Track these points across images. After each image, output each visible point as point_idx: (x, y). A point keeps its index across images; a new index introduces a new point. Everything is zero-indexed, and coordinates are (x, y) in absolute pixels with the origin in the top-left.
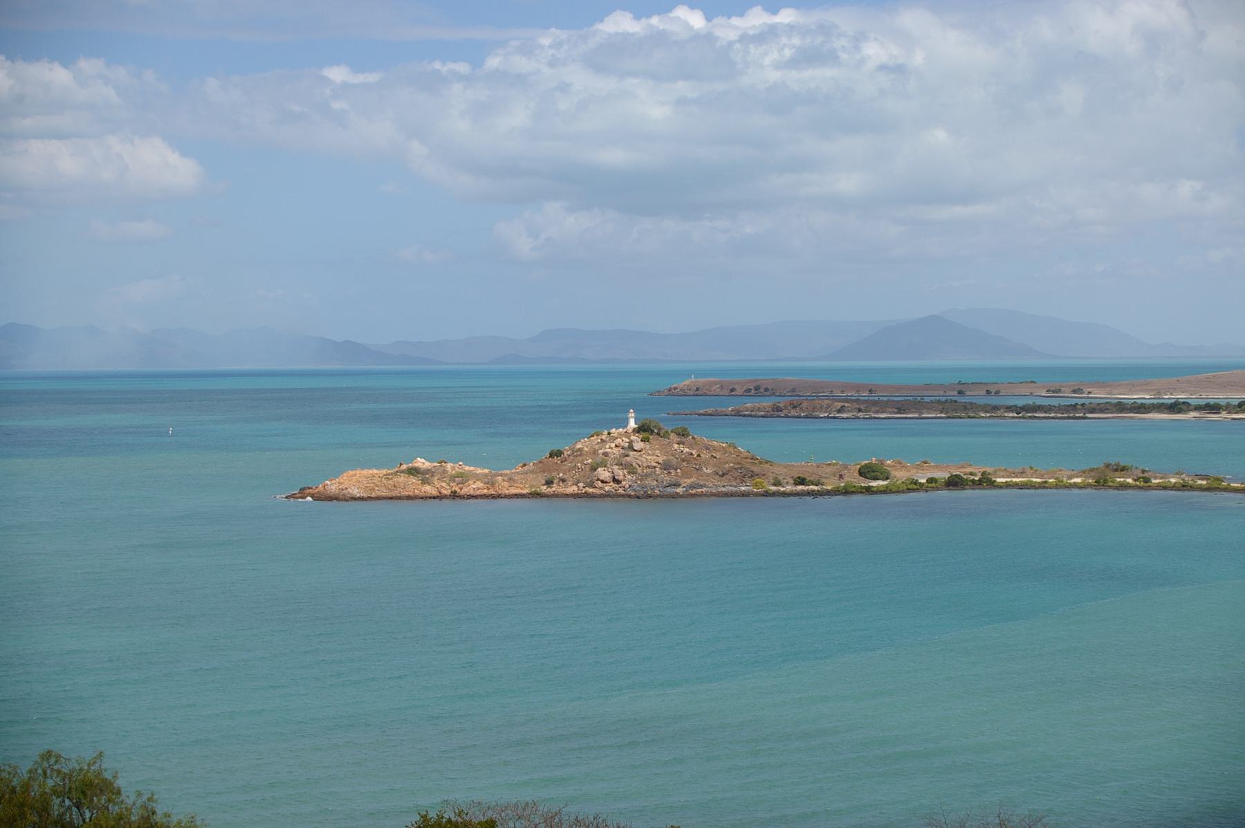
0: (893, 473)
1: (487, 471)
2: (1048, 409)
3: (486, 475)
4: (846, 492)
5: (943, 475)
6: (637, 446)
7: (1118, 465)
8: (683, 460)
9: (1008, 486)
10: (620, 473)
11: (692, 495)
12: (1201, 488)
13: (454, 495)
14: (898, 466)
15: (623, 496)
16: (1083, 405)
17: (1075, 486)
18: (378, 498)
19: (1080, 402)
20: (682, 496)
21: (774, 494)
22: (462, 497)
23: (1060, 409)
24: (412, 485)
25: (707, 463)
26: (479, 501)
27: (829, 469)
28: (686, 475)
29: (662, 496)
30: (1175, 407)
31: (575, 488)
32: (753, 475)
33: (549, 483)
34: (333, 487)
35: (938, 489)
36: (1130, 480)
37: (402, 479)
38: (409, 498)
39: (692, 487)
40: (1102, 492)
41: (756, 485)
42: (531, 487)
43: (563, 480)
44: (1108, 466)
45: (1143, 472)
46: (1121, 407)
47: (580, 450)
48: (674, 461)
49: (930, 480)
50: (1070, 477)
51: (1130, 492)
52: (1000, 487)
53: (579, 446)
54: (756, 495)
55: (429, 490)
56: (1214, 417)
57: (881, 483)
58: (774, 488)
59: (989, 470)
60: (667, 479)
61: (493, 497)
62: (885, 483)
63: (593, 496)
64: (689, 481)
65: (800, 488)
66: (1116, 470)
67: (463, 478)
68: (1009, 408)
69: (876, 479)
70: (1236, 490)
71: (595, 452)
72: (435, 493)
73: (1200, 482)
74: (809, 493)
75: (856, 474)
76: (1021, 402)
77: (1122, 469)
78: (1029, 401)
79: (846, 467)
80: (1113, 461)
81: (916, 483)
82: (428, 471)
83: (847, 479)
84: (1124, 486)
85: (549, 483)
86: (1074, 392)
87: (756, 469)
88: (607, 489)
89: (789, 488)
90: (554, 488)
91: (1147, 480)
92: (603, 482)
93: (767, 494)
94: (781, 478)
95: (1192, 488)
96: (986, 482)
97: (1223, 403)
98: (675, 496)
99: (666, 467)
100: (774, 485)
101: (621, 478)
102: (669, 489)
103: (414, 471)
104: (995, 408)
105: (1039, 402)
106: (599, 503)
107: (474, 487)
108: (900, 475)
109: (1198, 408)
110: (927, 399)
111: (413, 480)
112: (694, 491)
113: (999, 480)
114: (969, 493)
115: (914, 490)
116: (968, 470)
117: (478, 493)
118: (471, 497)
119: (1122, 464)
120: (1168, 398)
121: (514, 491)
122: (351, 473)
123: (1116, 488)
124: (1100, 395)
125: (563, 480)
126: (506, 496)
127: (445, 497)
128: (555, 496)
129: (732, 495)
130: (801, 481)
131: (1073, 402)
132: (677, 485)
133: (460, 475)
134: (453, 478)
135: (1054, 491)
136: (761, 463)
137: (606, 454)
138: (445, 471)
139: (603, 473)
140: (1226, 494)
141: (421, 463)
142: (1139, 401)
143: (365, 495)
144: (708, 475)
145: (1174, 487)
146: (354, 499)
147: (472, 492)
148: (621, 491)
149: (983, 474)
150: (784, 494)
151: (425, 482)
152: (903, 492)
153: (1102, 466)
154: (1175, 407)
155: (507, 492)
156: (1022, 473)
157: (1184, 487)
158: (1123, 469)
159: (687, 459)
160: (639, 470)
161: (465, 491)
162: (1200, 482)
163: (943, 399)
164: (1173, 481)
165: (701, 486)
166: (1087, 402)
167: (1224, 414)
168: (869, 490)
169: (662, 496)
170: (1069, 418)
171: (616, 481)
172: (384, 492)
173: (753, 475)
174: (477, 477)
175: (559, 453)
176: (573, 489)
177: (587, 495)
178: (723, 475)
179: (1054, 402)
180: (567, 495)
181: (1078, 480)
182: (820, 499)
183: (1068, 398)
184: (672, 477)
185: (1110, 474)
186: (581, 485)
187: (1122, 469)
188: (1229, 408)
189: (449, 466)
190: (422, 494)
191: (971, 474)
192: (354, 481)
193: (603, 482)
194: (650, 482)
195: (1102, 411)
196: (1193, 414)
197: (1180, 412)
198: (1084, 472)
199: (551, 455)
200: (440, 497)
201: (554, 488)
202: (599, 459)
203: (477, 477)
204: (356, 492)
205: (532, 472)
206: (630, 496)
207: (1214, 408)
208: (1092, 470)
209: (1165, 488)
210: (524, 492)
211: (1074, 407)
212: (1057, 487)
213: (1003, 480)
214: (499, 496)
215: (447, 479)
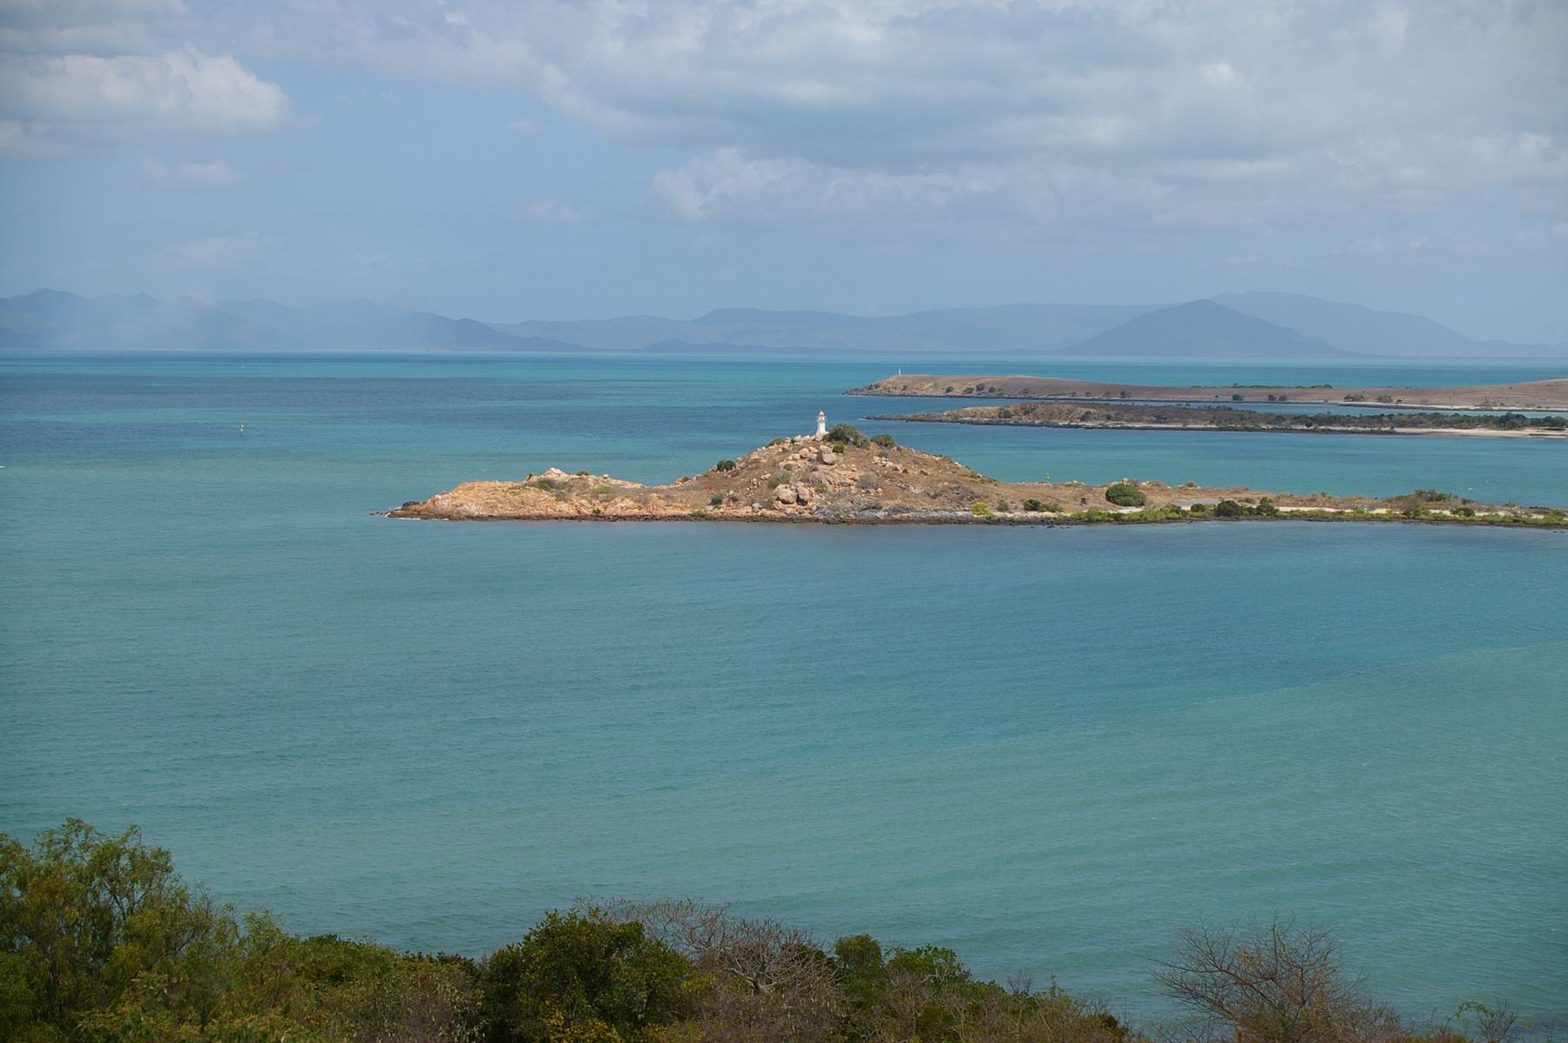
0: (1150, 497)
1: (638, 486)
2: (1347, 421)
3: (637, 491)
4: (1090, 520)
5: (1212, 501)
6: (828, 458)
7: (1432, 493)
8: (886, 477)
9: (1293, 516)
10: (806, 492)
11: (897, 521)
12: (1537, 525)
13: (597, 516)
15: (809, 520)
17: (1379, 518)
18: (501, 518)
19: (1387, 412)
20: (883, 522)
21: (999, 521)
22: (607, 518)
23: (1362, 421)
24: (544, 502)
25: (915, 481)
27: (1069, 492)
34: (444, 502)
36: (1447, 513)
37: (532, 494)
38: (540, 518)
39: (896, 510)
41: (976, 510)
42: (694, 506)
43: (735, 500)
44: (1420, 494)
45: (1464, 502)
47: (756, 461)
48: (874, 478)
49: (1196, 508)
50: (1373, 507)
51: (1447, 527)
52: (1284, 517)
53: (755, 456)
54: (977, 522)
55: (565, 508)
57: (1134, 510)
58: (999, 514)
59: (1270, 496)
60: (865, 500)
61: (646, 518)
62: (1139, 510)
63: (772, 520)
64: (892, 503)
65: (1032, 514)
66: (1431, 500)
67: (609, 494)
68: (1297, 419)
69: (1127, 504)
71: (775, 465)
72: (573, 512)
73: (1535, 516)
74: (1043, 521)
75: (1103, 499)
76: (1312, 412)
77: (1438, 499)
78: (1323, 411)
81: (1178, 510)
82: (564, 484)
83: (1090, 504)
85: (716, 502)
86: (1380, 400)
87: (977, 490)
88: (789, 511)
89: (1018, 514)
90: (723, 509)
91: (1469, 513)
92: (784, 502)
93: (990, 521)
94: (1008, 501)
95: (1526, 524)
96: (1265, 511)
98: (875, 522)
99: (864, 485)
100: (1000, 510)
101: (807, 497)
102: (867, 513)
103: (546, 485)
104: (1280, 418)
105: (1335, 412)
106: (778, 527)
107: (622, 505)
108: (1158, 501)
109: (1535, 423)
110: (1194, 406)
111: (545, 495)
112: (898, 516)
113: (1282, 509)
114: (1099, 527)
115: (1175, 520)
116: (1244, 495)
117: (627, 513)
118: (617, 518)
119: (1438, 492)
120: (1497, 412)
121: (671, 511)
122: (468, 485)
123: (1430, 522)
124: (1412, 404)
125: (735, 500)
126: (662, 518)
128: (724, 518)
129: (946, 521)
130: (1033, 506)
131: (1378, 412)
132: (877, 508)
133: (606, 490)
134: (595, 494)
135: (1352, 524)
137: (788, 467)
138: (585, 485)
139: (785, 492)
141: (556, 474)
142: (1461, 413)
144: (916, 496)
145: (1503, 523)
146: (471, 517)
147: (619, 512)
148: (806, 514)
149: (1263, 500)
150: (1012, 522)
151: (560, 498)
152: (1161, 522)
153: (1412, 492)
154: (1507, 422)
155: (663, 513)
156: (1312, 501)
157: (1516, 522)
158: (1439, 498)
160: (830, 488)
161: (611, 511)
162: (1535, 516)
163: (1215, 406)
164: (1502, 514)
165: (908, 510)
166: (1395, 412)
168: (1118, 518)
169: (858, 522)
171: (800, 501)
172: (509, 511)
174: (626, 494)
175: (725, 466)
176: (745, 511)
177: (763, 519)
178: (935, 497)
181: (1383, 511)
185: (1423, 504)
186: (756, 505)
187: (1438, 499)
189: (591, 478)
190: (556, 514)
191: (1248, 501)
192: (471, 498)
193: (784, 502)
194: (842, 503)
195: (1414, 425)
196: (1528, 431)
197: (1512, 427)
198: (1390, 501)
199: (719, 468)
200: (580, 518)
201: (723, 509)
202: (780, 473)
203: (626, 494)
204: (474, 509)
205: (695, 488)
208: (1400, 498)
209: (1491, 523)
210: (685, 513)
211: (1379, 419)
212: (1355, 519)
214: (654, 518)
215: (588, 496)
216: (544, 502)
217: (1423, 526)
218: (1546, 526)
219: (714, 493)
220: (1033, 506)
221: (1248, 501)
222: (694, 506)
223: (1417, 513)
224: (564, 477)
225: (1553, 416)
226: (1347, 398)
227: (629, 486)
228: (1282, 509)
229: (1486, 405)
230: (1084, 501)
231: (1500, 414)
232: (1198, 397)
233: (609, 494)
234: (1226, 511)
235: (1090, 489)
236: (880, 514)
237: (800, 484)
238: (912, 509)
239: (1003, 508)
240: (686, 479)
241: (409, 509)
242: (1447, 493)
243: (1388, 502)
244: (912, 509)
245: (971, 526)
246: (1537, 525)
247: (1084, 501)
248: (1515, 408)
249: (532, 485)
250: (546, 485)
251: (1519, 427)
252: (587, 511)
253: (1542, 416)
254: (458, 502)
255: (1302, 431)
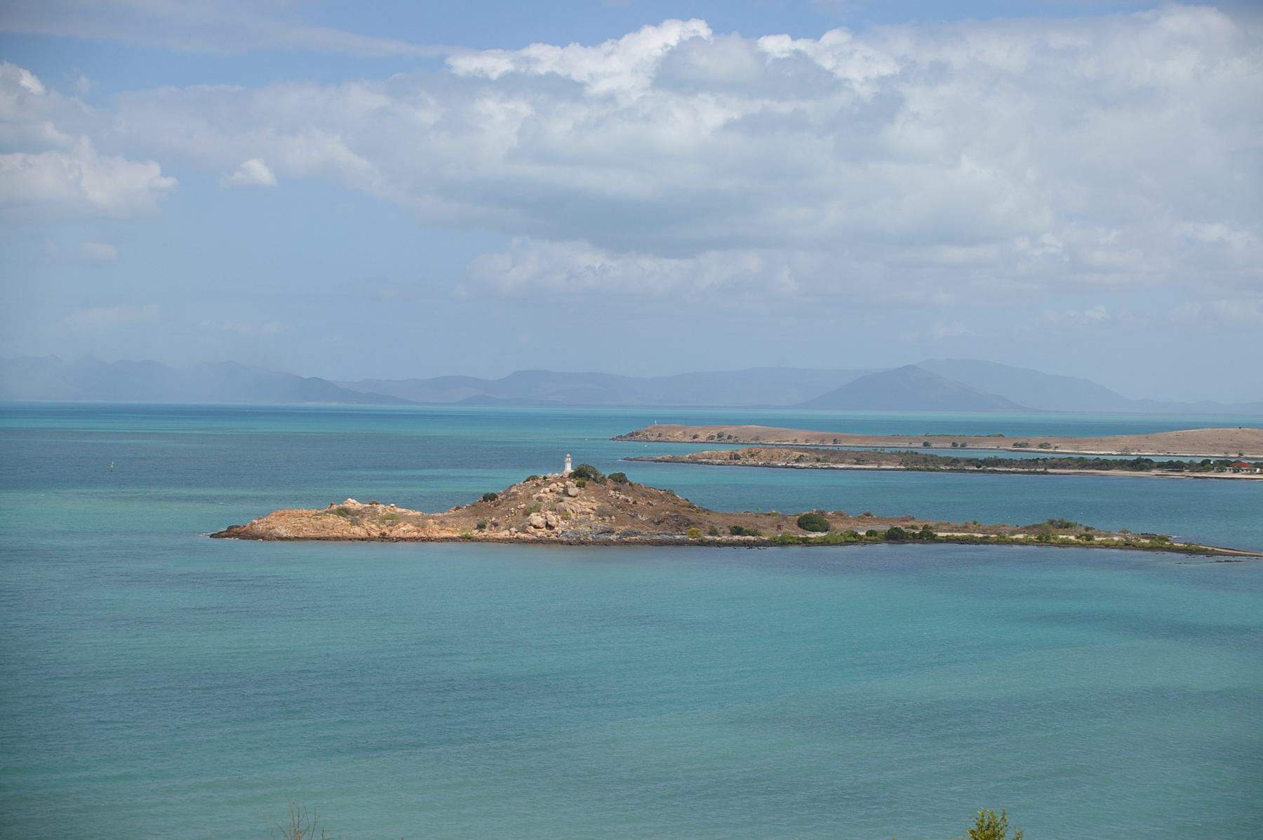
0: (833, 525)
1: (418, 513)
3: (417, 518)
4: (783, 543)
5: (883, 528)
6: (572, 491)
7: (1062, 522)
8: (618, 507)
9: (948, 540)
10: (553, 519)
11: (626, 543)
12: (1143, 548)
13: (383, 537)
14: (839, 518)
15: (555, 542)
16: (1044, 460)
17: (1017, 542)
18: (305, 539)
19: (1042, 456)
20: (615, 544)
21: (709, 544)
22: (391, 540)
23: (1021, 463)
24: (340, 526)
25: (643, 510)
26: (408, 544)
27: (768, 520)
28: (620, 522)
29: (594, 543)
30: (1140, 464)
31: (507, 533)
32: (689, 524)
33: (481, 527)
34: (260, 527)
35: (876, 542)
36: (1072, 538)
37: (331, 519)
38: (337, 539)
39: (626, 534)
40: (1044, 549)
43: (496, 525)
44: (1051, 522)
45: (1087, 529)
46: (1083, 463)
47: (514, 494)
48: (609, 507)
52: (941, 541)
55: (358, 531)
56: (1177, 475)
57: (820, 534)
59: (931, 524)
60: (601, 525)
61: (423, 540)
62: (824, 534)
63: (525, 542)
64: (623, 528)
65: (736, 537)
67: (394, 520)
68: (970, 461)
70: (1178, 550)
71: (529, 497)
72: (364, 534)
73: (1143, 541)
74: (745, 544)
75: (795, 525)
79: (785, 518)
80: (1057, 518)
81: (855, 535)
83: (785, 530)
84: (1066, 544)
85: (481, 527)
86: (1041, 446)
87: (692, 517)
88: (539, 534)
89: (725, 538)
90: (486, 532)
91: (1089, 538)
92: (535, 527)
94: (717, 527)
95: (1135, 547)
96: (927, 536)
97: (1186, 461)
98: (608, 543)
99: (601, 513)
100: (711, 534)
101: (554, 523)
102: (602, 536)
103: (344, 512)
104: (956, 461)
105: (1000, 456)
106: (530, 549)
108: (840, 527)
109: (1161, 466)
110: (887, 451)
111: (342, 520)
112: (627, 539)
113: (940, 534)
115: (852, 543)
116: (909, 524)
117: (408, 535)
119: (1067, 520)
120: (1134, 455)
121: (444, 534)
123: (1058, 545)
124: (1066, 450)
125: (496, 525)
126: (436, 540)
127: (373, 539)
128: (486, 540)
130: (738, 531)
131: (1034, 456)
132: (611, 532)
133: (392, 517)
134: (383, 520)
136: (698, 511)
137: (540, 499)
138: (375, 513)
139: (537, 519)
140: (1168, 554)
141: (352, 504)
142: (1102, 458)
143: (292, 535)
144: (643, 522)
146: (281, 538)
147: (402, 535)
148: (553, 537)
149: (925, 527)
150: (720, 544)
151: (354, 523)
152: (841, 544)
155: (437, 535)
156: (965, 528)
157: (1127, 545)
159: (623, 506)
160: (573, 516)
161: (395, 533)
162: (1143, 541)
163: (904, 451)
164: (1116, 539)
165: (636, 534)
167: (1187, 473)
168: (806, 542)
170: (1029, 473)
171: (549, 526)
173: (689, 524)
174: (408, 519)
176: (504, 534)
177: (519, 541)
178: (659, 523)
179: (1017, 456)
180: (498, 540)
181: (1020, 536)
182: (755, 549)
183: (1034, 452)
184: (606, 524)
185: (1054, 531)
186: (513, 529)
187: (1066, 526)
188: (1192, 467)
189: (380, 507)
191: (913, 527)
193: (535, 527)
194: (583, 528)
195: (1063, 467)
196: (1155, 472)
197: (1141, 470)
198: (1027, 528)
200: (369, 539)
201: (486, 532)
202: (532, 504)
204: (283, 532)
205: (465, 515)
206: (562, 542)
207: (1177, 466)
208: (1035, 526)
209: (1107, 546)
210: (455, 536)
211: (1035, 462)
212: (998, 542)
213: (945, 534)
214: (429, 539)
215: (377, 521)
216: (340, 526)
217: (1053, 549)
218: (1151, 548)
219: (480, 519)
220: (738, 531)
221: (913, 527)
222: (463, 530)
223: (1048, 538)
224: (359, 506)
225: (1175, 460)
226: (1015, 445)
227: (411, 513)
228: (940, 534)
229: (1126, 451)
230: (779, 527)
231: (1132, 459)
232: (891, 444)
233: (394, 520)
234: (895, 536)
235: (785, 518)
236: (613, 537)
237: (549, 513)
238: (639, 533)
239: (713, 532)
240: (458, 508)
241: (232, 532)
242: (1073, 521)
243: (1026, 529)
244: (639, 533)
245: (687, 548)
246: (1143, 548)
247: (779, 527)
248: (1147, 453)
249: (332, 512)
250: (344, 512)
251: (1148, 469)
252: (375, 534)
253: (1166, 460)
254: (271, 525)
255: (974, 471)
